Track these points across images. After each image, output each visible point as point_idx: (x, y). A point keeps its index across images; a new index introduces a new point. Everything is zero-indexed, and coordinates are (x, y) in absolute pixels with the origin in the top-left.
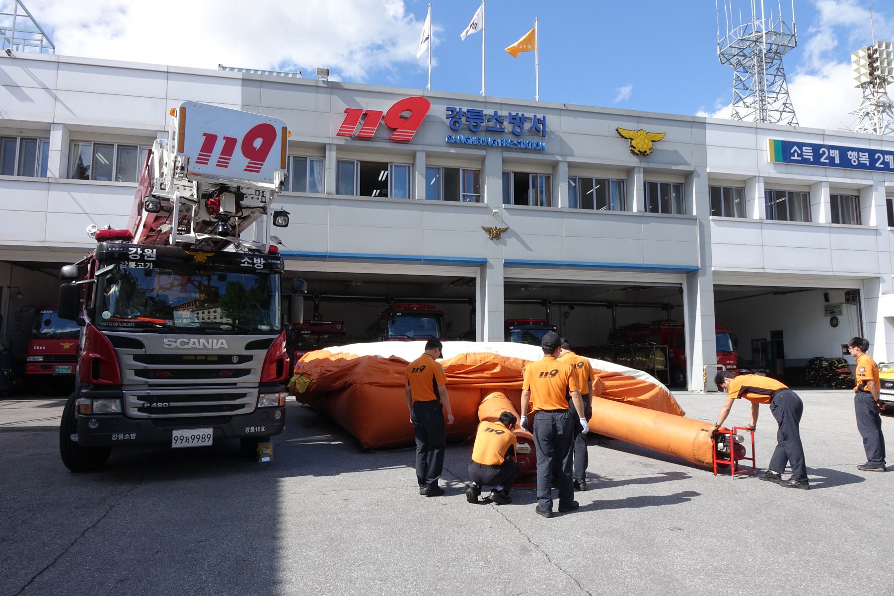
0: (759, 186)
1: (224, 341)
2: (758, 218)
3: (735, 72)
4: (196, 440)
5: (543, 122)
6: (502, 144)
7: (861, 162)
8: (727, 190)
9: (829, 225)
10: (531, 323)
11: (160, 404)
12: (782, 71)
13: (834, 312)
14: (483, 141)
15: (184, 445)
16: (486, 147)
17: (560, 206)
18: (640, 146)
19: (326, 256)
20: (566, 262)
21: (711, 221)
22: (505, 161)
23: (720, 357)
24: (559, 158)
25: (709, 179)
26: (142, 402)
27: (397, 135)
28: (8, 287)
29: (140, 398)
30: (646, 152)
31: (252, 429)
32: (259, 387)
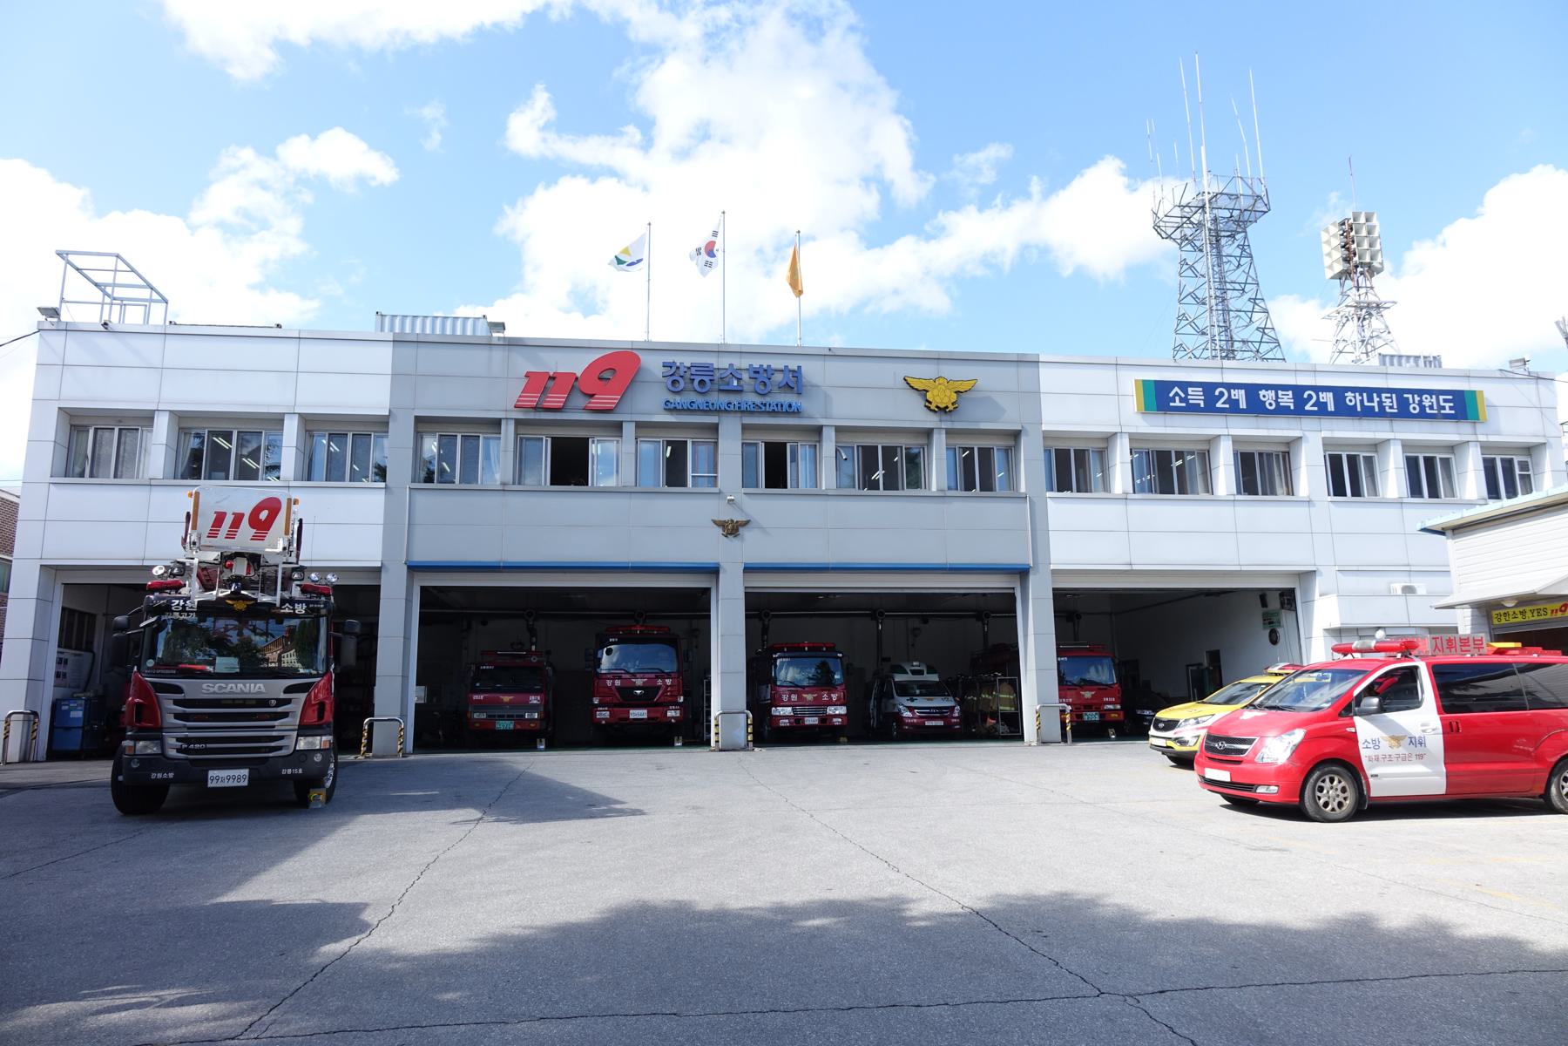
0: (1121, 444)
1: (261, 685)
2: (1121, 492)
5: (797, 374)
6: (739, 408)
7: (1281, 404)
8: (1081, 455)
9: (1232, 498)
10: (806, 648)
13: (1272, 623)
16: (719, 411)
17: (824, 488)
20: (833, 564)
21: (1048, 500)
22: (745, 428)
24: (822, 422)
25: (1045, 438)
26: (180, 744)
27: (596, 402)
28: (104, 615)
29: (178, 740)
30: (947, 407)
31: (289, 771)
32: (298, 730)
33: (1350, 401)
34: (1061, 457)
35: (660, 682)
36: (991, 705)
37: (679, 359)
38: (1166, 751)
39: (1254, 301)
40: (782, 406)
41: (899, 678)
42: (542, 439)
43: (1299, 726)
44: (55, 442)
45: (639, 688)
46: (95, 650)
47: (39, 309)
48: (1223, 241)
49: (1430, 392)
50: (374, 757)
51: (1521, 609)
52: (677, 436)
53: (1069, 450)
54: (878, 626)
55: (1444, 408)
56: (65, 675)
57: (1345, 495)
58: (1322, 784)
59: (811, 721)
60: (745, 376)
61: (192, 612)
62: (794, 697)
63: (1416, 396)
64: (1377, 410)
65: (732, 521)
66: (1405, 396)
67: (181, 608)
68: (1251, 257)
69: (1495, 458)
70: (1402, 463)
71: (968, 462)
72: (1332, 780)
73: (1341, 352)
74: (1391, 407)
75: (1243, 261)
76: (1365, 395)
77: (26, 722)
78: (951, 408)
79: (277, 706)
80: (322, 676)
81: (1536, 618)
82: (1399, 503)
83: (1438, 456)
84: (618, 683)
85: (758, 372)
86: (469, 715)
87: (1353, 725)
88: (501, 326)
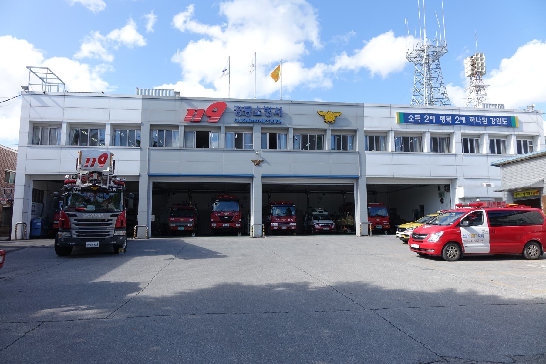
1: (102, 215)
2: (391, 151)
3: (415, 67)
4: (94, 245)
5: (280, 110)
6: (260, 121)
7: (447, 121)
8: (377, 138)
9: (429, 153)
11: (82, 234)
12: (439, 66)
13: (442, 196)
14: (251, 120)
15: (90, 246)
16: (253, 123)
17: (289, 149)
18: (328, 119)
19: (179, 175)
21: (366, 154)
22: (262, 128)
23: (380, 219)
24: (289, 126)
27: (211, 120)
29: (76, 232)
30: (332, 122)
31: (112, 242)
32: (115, 229)
33: (471, 120)
34: (371, 139)
35: (233, 214)
36: (345, 223)
37: (239, 105)
38: (402, 238)
39: (441, 84)
40: (275, 121)
41: (314, 213)
42: (193, 132)
43: (442, 230)
44: (29, 132)
45: (226, 216)
46: (44, 202)
47: (22, 87)
48: (431, 62)
49: (499, 117)
50: (138, 238)
51: (523, 192)
52: (239, 131)
53: (374, 136)
54: (308, 196)
55: (504, 123)
56: (34, 211)
57: (468, 153)
58: (449, 249)
59: (284, 228)
60: (263, 111)
61: (79, 190)
62: (278, 220)
63: (494, 118)
64: (480, 123)
65: (258, 160)
66: (491, 118)
67: (76, 189)
68: (440, 68)
69: (521, 140)
70: (488, 142)
71: (339, 140)
72: (452, 248)
73: (470, 102)
74: (485, 122)
75: (437, 70)
76: (476, 118)
77: (22, 226)
78: (333, 122)
79: (108, 221)
80: (122, 212)
81: (528, 195)
82: (487, 155)
83: (501, 139)
84: (219, 214)
85: (267, 109)
86: (169, 225)
87: (460, 230)
88: (179, 93)
